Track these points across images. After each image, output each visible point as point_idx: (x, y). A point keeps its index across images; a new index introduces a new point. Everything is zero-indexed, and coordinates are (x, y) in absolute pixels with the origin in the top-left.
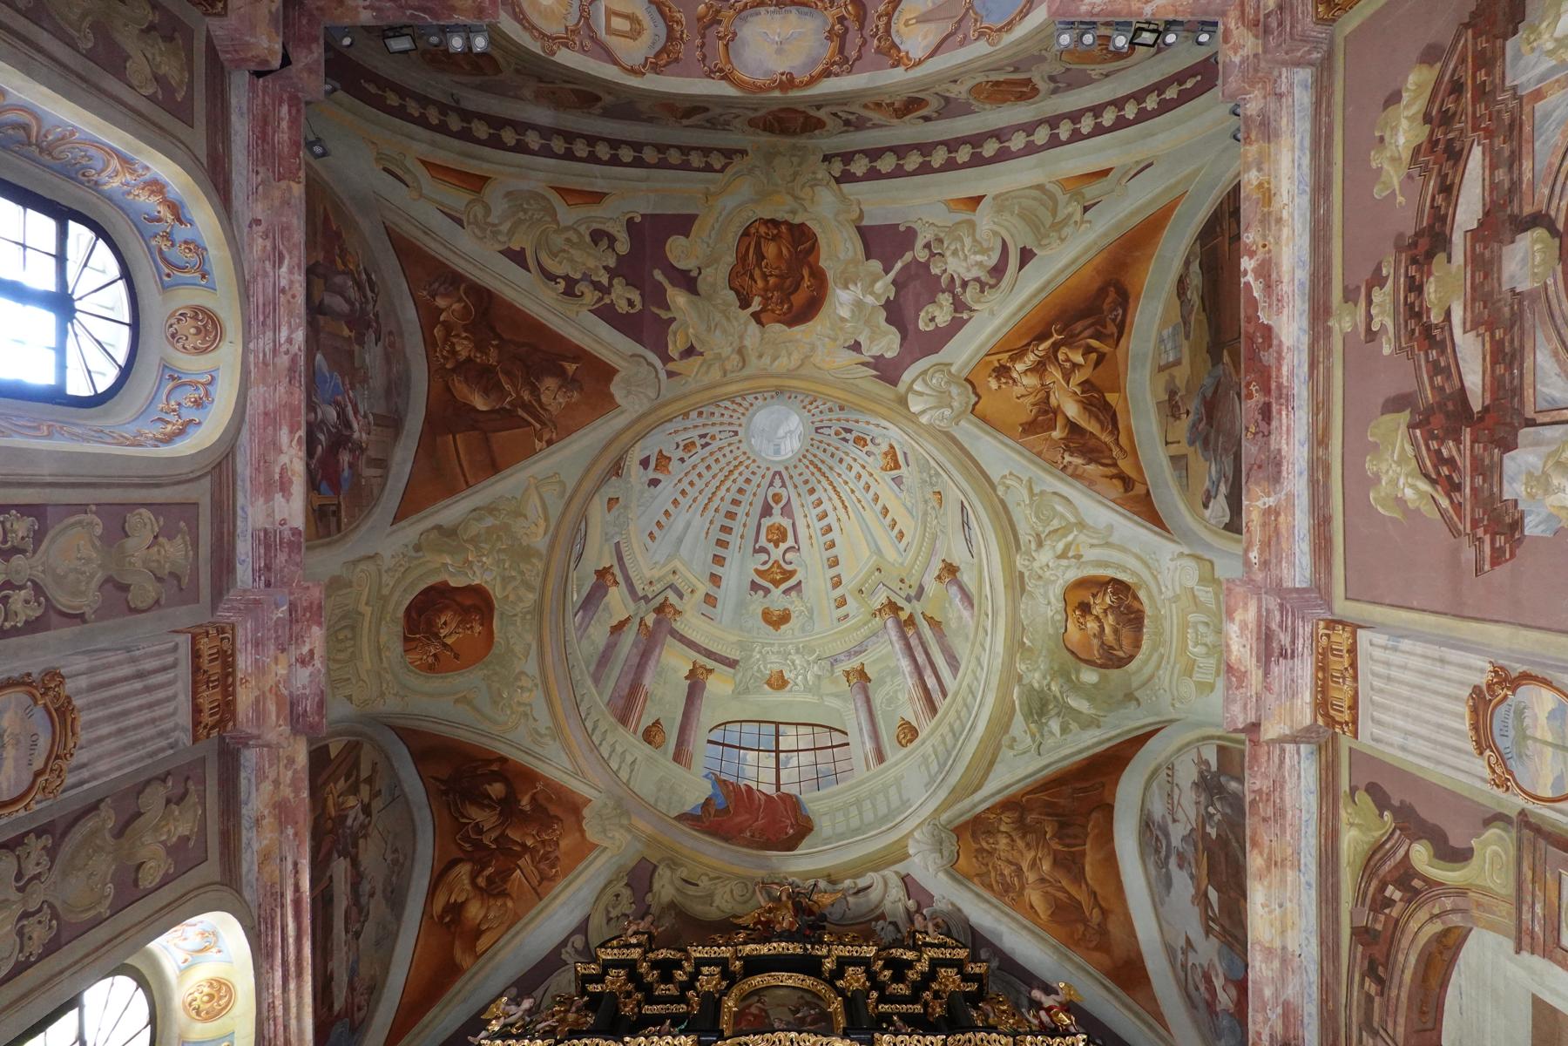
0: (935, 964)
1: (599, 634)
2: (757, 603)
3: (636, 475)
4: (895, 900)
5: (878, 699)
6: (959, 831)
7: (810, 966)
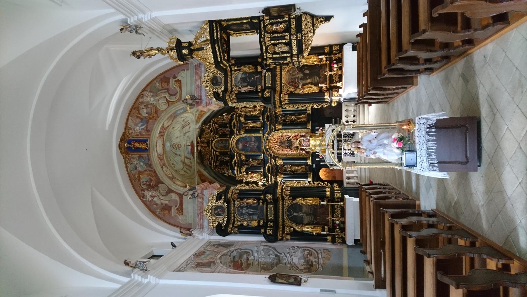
1: (188, 171)
4: (198, 130)
7: (212, 141)
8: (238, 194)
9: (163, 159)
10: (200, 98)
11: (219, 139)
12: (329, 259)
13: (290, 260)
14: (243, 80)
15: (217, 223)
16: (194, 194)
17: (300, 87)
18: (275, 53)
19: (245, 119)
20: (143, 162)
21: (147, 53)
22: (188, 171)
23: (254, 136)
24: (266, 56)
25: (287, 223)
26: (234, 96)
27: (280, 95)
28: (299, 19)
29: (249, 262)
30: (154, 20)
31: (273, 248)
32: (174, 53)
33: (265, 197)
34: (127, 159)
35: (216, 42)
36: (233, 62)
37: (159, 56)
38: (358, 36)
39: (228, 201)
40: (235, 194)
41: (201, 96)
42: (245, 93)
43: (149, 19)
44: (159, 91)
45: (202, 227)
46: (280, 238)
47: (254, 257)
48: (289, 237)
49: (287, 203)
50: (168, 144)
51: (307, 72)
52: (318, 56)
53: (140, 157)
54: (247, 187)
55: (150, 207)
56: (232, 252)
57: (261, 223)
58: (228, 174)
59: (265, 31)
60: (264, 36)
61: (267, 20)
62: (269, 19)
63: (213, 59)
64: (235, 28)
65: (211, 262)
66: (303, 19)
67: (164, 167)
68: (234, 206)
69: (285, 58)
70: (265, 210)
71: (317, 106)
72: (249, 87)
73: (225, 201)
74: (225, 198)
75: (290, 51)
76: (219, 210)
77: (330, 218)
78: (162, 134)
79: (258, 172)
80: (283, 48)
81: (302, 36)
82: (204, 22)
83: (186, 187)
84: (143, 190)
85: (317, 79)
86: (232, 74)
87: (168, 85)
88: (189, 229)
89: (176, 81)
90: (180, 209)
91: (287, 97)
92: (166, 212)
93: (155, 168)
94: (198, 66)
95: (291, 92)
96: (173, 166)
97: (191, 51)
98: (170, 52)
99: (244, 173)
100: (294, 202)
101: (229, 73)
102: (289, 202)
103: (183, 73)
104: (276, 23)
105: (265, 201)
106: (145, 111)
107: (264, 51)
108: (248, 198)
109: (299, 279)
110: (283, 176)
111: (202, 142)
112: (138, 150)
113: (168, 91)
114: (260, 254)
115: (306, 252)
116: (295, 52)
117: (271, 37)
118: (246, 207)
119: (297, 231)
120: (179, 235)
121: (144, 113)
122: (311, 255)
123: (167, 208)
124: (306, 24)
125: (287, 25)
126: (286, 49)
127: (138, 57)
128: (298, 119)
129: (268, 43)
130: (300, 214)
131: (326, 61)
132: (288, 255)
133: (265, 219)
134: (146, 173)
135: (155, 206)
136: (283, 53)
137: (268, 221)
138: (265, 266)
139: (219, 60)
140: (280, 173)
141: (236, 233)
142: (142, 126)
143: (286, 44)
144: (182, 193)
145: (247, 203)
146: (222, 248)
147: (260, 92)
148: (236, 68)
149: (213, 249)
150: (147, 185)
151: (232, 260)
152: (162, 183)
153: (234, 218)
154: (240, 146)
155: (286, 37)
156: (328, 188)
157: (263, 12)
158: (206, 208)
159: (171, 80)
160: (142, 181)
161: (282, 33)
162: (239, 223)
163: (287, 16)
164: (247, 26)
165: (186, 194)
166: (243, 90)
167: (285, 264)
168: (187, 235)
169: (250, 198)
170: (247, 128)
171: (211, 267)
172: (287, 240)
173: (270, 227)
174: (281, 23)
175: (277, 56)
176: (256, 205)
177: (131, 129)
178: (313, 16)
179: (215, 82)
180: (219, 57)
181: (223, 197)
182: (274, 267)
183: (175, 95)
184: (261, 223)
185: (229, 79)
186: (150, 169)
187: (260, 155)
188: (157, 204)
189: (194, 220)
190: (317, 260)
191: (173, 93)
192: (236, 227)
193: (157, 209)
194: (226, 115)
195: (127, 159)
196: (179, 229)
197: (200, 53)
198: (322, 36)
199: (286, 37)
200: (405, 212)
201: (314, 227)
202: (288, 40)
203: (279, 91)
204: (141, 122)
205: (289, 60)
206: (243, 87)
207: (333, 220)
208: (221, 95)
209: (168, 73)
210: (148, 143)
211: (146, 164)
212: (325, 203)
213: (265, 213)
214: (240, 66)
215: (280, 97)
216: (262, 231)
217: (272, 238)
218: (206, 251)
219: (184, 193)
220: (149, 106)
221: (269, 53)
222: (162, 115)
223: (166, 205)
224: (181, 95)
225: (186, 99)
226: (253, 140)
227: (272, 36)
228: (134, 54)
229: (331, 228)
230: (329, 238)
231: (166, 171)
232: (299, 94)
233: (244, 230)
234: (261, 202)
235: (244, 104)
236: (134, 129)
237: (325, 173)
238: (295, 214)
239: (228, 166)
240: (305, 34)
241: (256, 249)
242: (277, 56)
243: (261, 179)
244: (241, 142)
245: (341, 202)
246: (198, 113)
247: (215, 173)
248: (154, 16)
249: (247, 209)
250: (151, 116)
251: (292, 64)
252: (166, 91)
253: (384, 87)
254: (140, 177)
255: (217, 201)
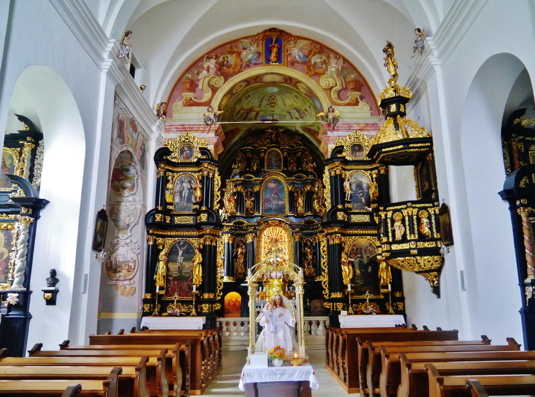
0: (298, 149)
1: (239, 115)
2: (269, 106)
3: (243, 99)
4: (293, 129)
5: (292, 115)
6: (305, 128)
7: (279, 148)
8: (208, 177)
9: (256, 82)
10: (335, 128)
11: (282, 156)
12: (122, 294)
13: (122, 243)
14: (359, 186)
15: (171, 150)
16: (210, 120)
17: (350, 259)
18: (393, 221)
19: (308, 191)
20: (253, 57)
21: (390, 61)
22: (239, 115)
23: (285, 204)
24: (389, 210)
25: (169, 242)
26: (338, 172)
27: (339, 233)
28: (435, 251)
29: (121, 190)
30: (431, 69)
31: (138, 221)
32: (391, 94)
33: (204, 212)
34: (257, 38)
35: (405, 146)
36: (382, 172)
37: (387, 77)
38: (414, 326)
39: (198, 164)
40: (208, 173)
41: (338, 130)
42: (342, 188)
43: (433, 63)
44: (344, 78)
45: (167, 131)
46: (151, 231)
47: (128, 197)
48: (151, 243)
49: (195, 243)
50: (275, 90)
51: (370, 270)
52: (390, 283)
53: (259, 54)
54: (216, 189)
55: (196, 65)
56: (135, 168)
57: (170, 207)
58: (234, 168)
59: (420, 209)
60: (414, 208)
61: (435, 211)
62: (435, 214)
63: (384, 141)
64: (424, 171)
65: (123, 138)
66: (436, 258)
67: (246, 83)
68: (192, 172)
69: (386, 234)
70: (186, 213)
71: (325, 283)
72: (350, 192)
73: (199, 159)
74: (203, 159)
75: (395, 242)
76: (187, 152)
77: (176, 297)
78: (289, 82)
79: (236, 208)
80: (399, 231)
81: (414, 256)
82: (431, 132)
83: (219, 110)
84: (217, 57)
85: (360, 282)
86: (367, 170)
87: (352, 89)
88: (165, 114)
89: (357, 99)
90: (191, 103)
91: (337, 241)
92: (188, 86)
93: (245, 72)
94: (375, 127)
95: (343, 249)
96: (247, 95)
97: (394, 116)
98: (393, 89)
99: (235, 190)
100: (197, 251)
101: (368, 167)
102: (196, 244)
103: (367, 108)
104: (430, 223)
105: (198, 212)
106: (318, 61)
107: (396, 207)
108: (202, 189)
109: (100, 248)
110: (231, 242)
111: (277, 135)
112: (269, 51)
113: (345, 89)
114: (131, 205)
115: (132, 264)
116: (395, 247)
117: (412, 216)
118: (191, 188)
119: (158, 254)
120: (159, 101)
121: (316, 59)
122: (129, 271)
123: (193, 86)
124: (429, 262)
125: (428, 236)
126: (399, 236)
127: (385, 51)
128: (308, 264)
129: (405, 212)
130: (180, 259)
131: (383, 294)
132: (128, 241)
133: (175, 213)
134: (239, 61)
135: (196, 72)
136: (394, 232)
137: (172, 216)
138: (116, 211)
139: (383, 150)
140: (234, 239)
141: (158, 173)
142: (300, 57)
143: (404, 236)
144: (212, 104)
145: (195, 189)
146: (141, 154)
147: (344, 206)
148: (374, 176)
149: (140, 144)
150: (223, 62)
151: (125, 167)
152: (226, 80)
153: (177, 172)
154: (272, 185)
155: (413, 235)
156: (215, 296)
157: (444, 205)
158: (191, 134)
159: (358, 93)
160: (229, 56)
161: (418, 230)
162: (170, 178)
163: (439, 236)
164: (427, 188)
165: (210, 109)
166: (346, 184)
167: (117, 237)
168: (158, 111)
169: (202, 193)
170: (296, 194)
171: (118, 139)
172: (148, 241)
173: (165, 219)
174: (431, 229)
175: (389, 225)
176: (193, 200)
177: (295, 43)
178: (439, 270)
179: (357, 148)
180: (387, 149)
181: (204, 157)
182: (114, 222)
183: (339, 98)
184: (170, 207)
185: (361, 167)
186: (244, 65)
187: (259, 211)
188: (198, 74)
189: (176, 120)
190: (122, 278)
191: (341, 95)
192: (165, 173)
193: (192, 75)
194: (314, 167)
195: (257, 38)
196: (165, 100)
197: (392, 126)
198: (415, 285)
199: (413, 235)
200: (188, 369)
201: (164, 277)
202: (409, 238)
203: (345, 232)
204: (304, 56)
205: (385, 240)
206: (350, 185)
207: (173, 302)
208: (339, 156)
209: (368, 90)
210: (277, 64)
211: (250, 61)
212: (194, 290)
213: (182, 213)
214: (377, 181)
215: (335, 233)
216: (160, 208)
217: (151, 221)
218: (137, 134)
219: (211, 107)
220: (324, 66)
221: (393, 214)
222: (314, 82)
223: (197, 86)
224: (339, 105)
225: (333, 111)
226: (280, 203)
227: (415, 217)
228: (390, 46)
229: (163, 299)
230: (149, 296)
231: (241, 86)
232: (340, 258)
233: (162, 184)
234: (198, 206)
235: (328, 187)
236: (295, 47)
237: (234, 300)
238: (180, 252)
239: (246, 168)
240: (416, 260)
241: (137, 199)
242: (389, 225)
243: (226, 212)
244: (276, 186)
245: (196, 312)
246: (316, 129)
247: (236, 151)
248: (435, 69)
249: (189, 189)
250: (311, 68)
251: (379, 245)
252: (344, 86)
253: (346, 352)
254: (233, 53)
255: (200, 148)
